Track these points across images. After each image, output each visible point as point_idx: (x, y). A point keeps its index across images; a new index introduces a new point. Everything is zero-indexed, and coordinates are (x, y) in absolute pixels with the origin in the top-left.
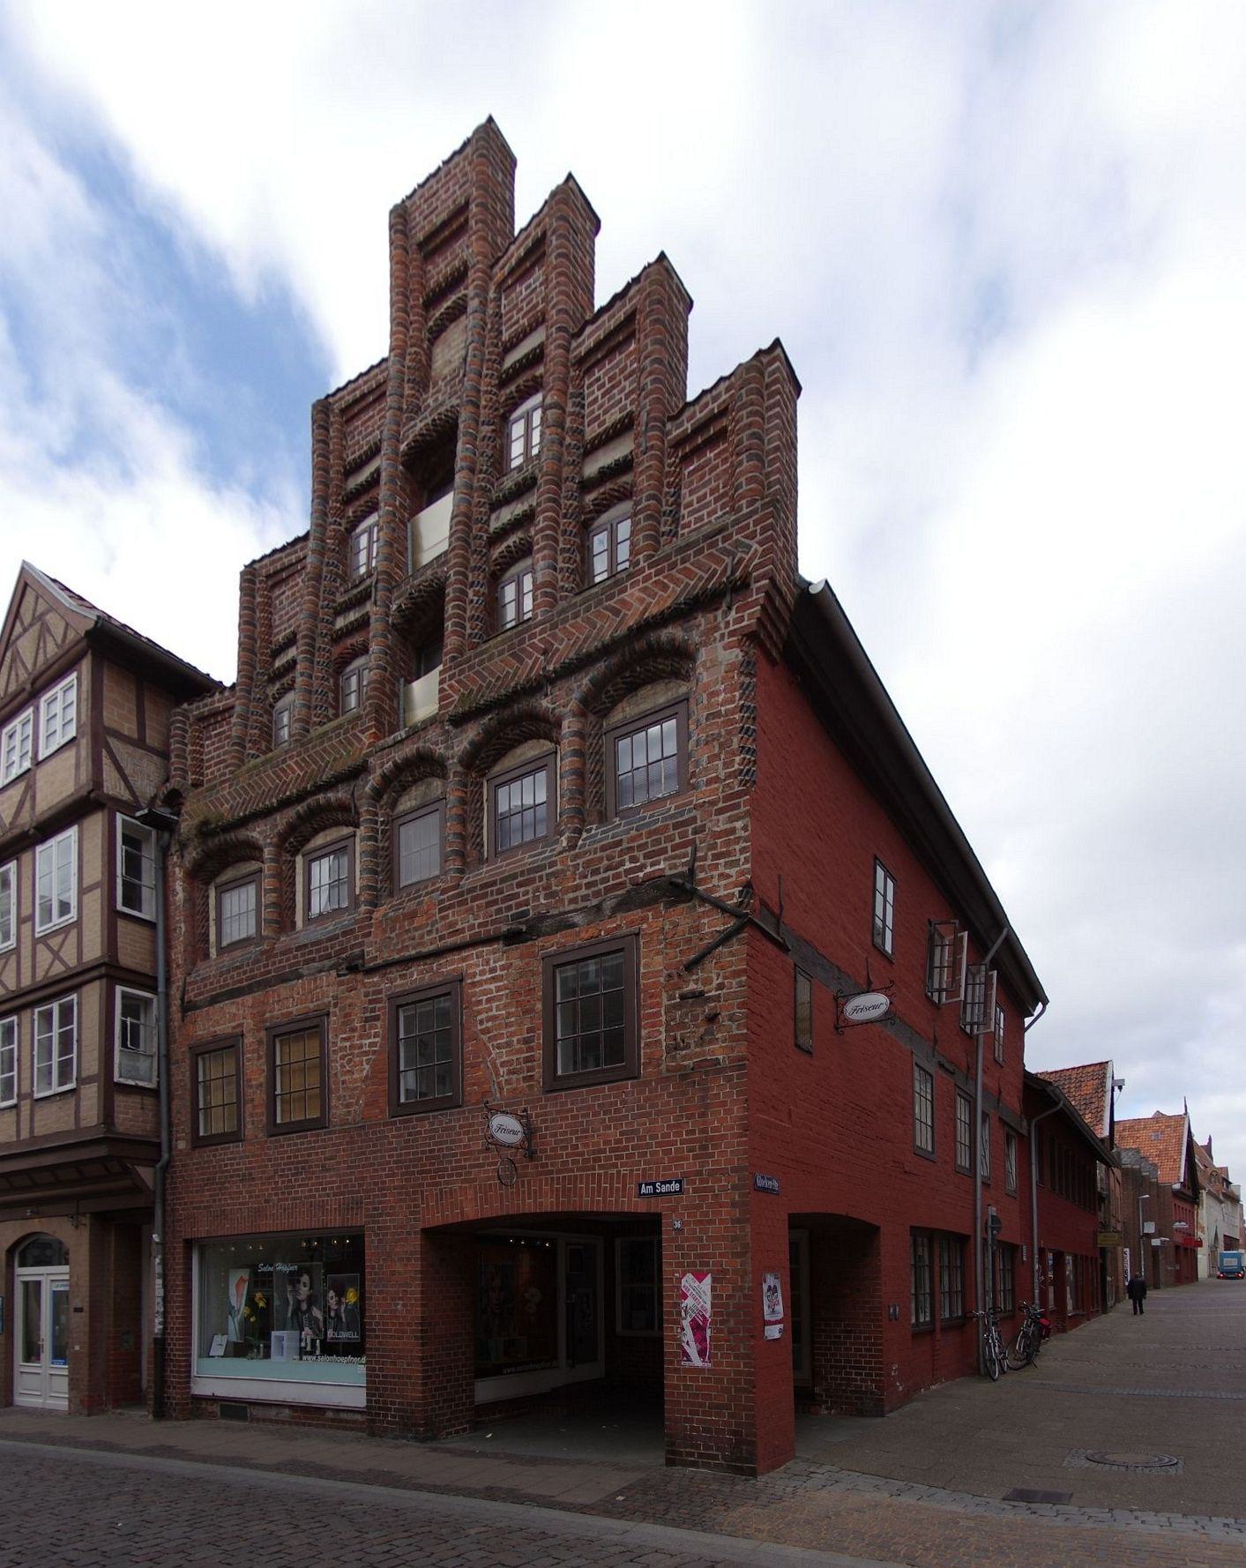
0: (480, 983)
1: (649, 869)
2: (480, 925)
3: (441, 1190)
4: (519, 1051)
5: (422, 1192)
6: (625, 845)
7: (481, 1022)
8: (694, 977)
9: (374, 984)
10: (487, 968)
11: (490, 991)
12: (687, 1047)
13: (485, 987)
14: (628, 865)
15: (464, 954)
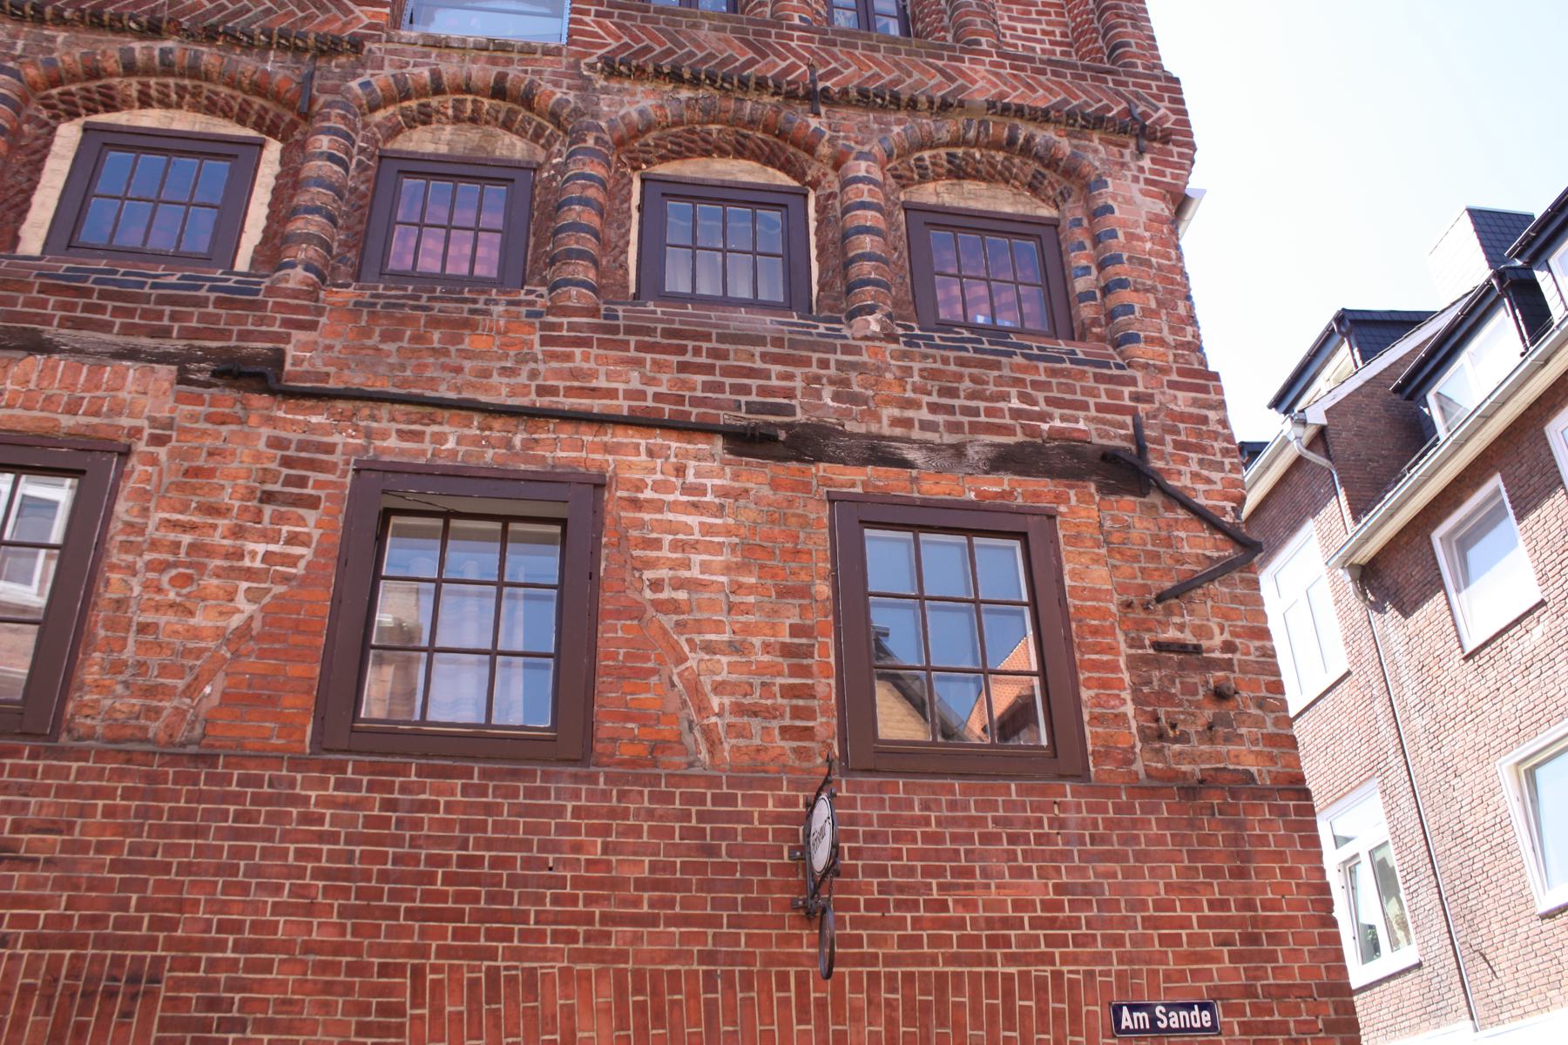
0: (658, 506)
1: (1057, 423)
2: (658, 397)
3: (493, 974)
4: (762, 669)
5: (418, 973)
6: (1006, 372)
7: (656, 585)
8: (1177, 620)
9: (313, 429)
10: (678, 483)
11: (688, 529)
12: (1183, 738)
13: (670, 516)
14: (1015, 403)
15: (611, 436)
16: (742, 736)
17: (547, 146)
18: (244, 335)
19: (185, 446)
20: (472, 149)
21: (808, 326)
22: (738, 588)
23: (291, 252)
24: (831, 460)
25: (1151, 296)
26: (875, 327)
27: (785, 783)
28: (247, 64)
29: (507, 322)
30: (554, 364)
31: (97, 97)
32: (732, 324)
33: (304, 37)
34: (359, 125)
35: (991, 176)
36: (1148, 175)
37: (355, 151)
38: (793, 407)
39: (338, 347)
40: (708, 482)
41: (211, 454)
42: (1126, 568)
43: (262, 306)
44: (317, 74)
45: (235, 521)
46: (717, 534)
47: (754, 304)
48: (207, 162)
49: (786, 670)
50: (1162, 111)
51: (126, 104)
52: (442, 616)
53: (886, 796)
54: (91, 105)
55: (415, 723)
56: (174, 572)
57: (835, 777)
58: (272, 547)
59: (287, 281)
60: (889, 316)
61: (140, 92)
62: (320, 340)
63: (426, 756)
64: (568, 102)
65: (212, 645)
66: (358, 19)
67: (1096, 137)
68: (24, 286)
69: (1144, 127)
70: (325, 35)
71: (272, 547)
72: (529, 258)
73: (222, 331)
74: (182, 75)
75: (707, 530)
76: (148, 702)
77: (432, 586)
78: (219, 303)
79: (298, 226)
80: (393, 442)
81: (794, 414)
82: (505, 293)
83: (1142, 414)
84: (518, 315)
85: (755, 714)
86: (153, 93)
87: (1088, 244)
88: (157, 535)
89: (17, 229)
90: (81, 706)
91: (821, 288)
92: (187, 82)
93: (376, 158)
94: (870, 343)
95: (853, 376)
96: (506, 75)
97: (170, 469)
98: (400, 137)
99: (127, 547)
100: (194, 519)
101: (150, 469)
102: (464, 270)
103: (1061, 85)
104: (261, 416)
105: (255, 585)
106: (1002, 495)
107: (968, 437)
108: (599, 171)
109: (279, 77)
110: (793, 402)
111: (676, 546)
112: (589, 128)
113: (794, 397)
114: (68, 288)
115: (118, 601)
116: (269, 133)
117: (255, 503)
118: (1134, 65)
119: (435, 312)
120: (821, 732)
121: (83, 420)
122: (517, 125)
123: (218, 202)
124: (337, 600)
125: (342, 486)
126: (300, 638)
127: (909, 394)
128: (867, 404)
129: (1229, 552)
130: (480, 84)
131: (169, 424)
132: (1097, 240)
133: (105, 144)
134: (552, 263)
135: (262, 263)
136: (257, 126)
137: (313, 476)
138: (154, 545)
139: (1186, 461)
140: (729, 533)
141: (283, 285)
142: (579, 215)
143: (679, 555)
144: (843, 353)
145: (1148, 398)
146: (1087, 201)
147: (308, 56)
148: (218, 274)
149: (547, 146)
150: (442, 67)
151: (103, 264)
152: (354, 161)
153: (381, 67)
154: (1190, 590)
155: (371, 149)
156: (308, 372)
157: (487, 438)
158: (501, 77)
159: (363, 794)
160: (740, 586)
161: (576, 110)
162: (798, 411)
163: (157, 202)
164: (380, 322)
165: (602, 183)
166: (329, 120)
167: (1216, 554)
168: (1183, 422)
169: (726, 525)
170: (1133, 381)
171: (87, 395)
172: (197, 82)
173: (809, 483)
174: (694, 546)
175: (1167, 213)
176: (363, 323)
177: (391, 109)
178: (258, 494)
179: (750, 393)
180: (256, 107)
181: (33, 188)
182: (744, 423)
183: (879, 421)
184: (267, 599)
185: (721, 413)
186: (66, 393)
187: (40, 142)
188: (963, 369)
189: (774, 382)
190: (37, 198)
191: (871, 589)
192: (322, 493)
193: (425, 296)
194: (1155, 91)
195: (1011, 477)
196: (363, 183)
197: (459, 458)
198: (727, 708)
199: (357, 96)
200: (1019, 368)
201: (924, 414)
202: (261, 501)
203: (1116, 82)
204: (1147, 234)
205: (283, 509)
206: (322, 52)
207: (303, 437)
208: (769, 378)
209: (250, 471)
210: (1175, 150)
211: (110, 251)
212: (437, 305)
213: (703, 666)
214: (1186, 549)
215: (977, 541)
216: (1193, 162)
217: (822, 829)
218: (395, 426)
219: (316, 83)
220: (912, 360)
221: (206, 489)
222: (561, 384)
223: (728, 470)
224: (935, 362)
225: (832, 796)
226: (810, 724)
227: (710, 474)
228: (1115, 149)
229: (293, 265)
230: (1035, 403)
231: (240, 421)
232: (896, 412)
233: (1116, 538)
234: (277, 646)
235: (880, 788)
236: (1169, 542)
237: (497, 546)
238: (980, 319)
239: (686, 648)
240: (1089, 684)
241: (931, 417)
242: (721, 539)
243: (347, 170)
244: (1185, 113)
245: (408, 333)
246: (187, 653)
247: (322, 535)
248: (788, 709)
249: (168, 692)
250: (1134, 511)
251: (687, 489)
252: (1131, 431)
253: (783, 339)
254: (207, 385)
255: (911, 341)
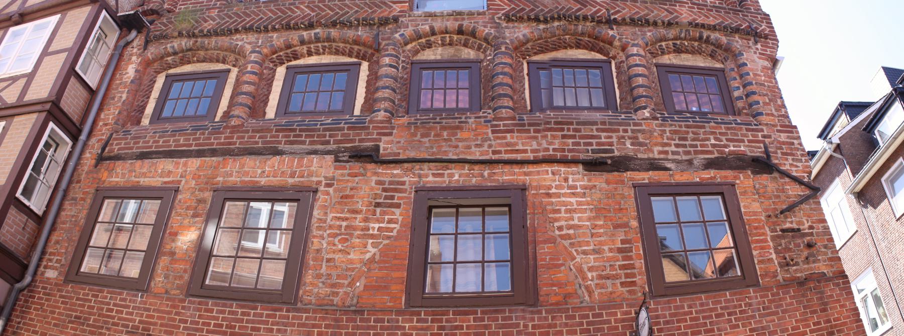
4: (609, 259)
8: (789, 220)
11: (571, 204)
16: (603, 288)
17: (484, 52)
18: (361, 141)
19: (341, 187)
20: (451, 56)
21: (617, 116)
22: (595, 226)
23: (378, 105)
24: (633, 170)
25: (766, 97)
26: (647, 115)
27: (625, 305)
28: (350, 34)
29: (476, 125)
30: (499, 141)
31: (291, 55)
32: (581, 117)
33: (373, 19)
34: (401, 52)
35: (693, 52)
36: (760, 51)
37: (400, 62)
38: (613, 150)
39: (402, 142)
40: (578, 184)
41: (351, 189)
42: (767, 202)
43: (368, 128)
44: (380, 33)
45: (364, 215)
46: (584, 205)
47: (591, 108)
48: (337, 74)
49: (621, 258)
50: (763, 27)
51: (303, 56)
52: (459, 249)
53: (672, 305)
54: (289, 59)
55: (450, 293)
56: (340, 237)
57: (647, 300)
58: (381, 225)
59: (377, 117)
60: (653, 109)
61: (308, 51)
62: (394, 139)
63: (456, 307)
64: (491, 33)
65: (358, 266)
66: (395, 9)
67: (737, 36)
68: (270, 131)
69: (756, 33)
70: (382, 17)
71: (381, 225)
72: (482, 98)
73: (351, 140)
74: (324, 42)
75: (579, 203)
76: (333, 290)
77: (454, 236)
78: (349, 128)
79: (379, 94)
80: (431, 178)
81: (614, 153)
82: (473, 114)
83: (767, 143)
84: (480, 122)
85: (608, 278)
86: (313, 50)
87: (738, 78)
88: (332, 223)
89: (265, 110)
90: (305, 292)
91: (621, 100)
92: (326, 44)
93: (410, 64)
94: (646, 121)
95: (639, 135)
96: (463, 25)
97: (335, 196)
98: (419, 54)
99: (319, 228)
100: (346, 215)
101: (326, 197)
102: (454, 105)
103: (719, 15)
104: (372, 172)
105: (375, 241)
106: (711, 178)
107: (693, 156)
108: (509, 61)
109: (364, 37)
110: (613, 148)
111: (567, 211)
112: (502, 43)
113: (613, 145)
114: (287, 129)
115: (317, 250)
116: (363, 59)
117: (373, 207)
118: (750, 9)
119: (444, 124)
120: (639, 282)
121: (297, 179)
122: (470, 45)
123: (344, 89)
124: (412, 245)
125: (410, 198)
126: (397, 262)
127: (666, 141)
128: (646, 146)
129: (808, 192)
130: (452, 30)
131: (333, 178)
132: (741, 76)
133: (296, 73)
134: (493, 99)
135: (365, 111)
136: (357, 57)
137: (397, 195)
138: (331, 227)
139: (787, 160)
140: (588, 204)
141: (376, 119)
142: (502, 79)
143: (568, 215)
144: (634, 126)
145: (769, 137)
146: (736, 61)
147: (376, 27)
148: (347, 117)
149: (484, 52)
150: (434, 24)
151: (299, 119)
152: (401, 66)
153: (408, 27)
154: (794, 208)
155: (407, 60)
156: (390, 153)
157: (472, 174)
158: (461, 26)
159: (429, 324)
160: (596, 226)
161: (495, 37)
162: (616, 151)
163: (319, 92)
164: (420, 130)
165: (511, 65)
166: (388, 51)
167: (802, 194)
168: (784, 145)
169: (587, 201)
170: (762, 130)
171: (298, 170)
172: (330, 43)
173: (624, 180)
174: (575, 211)
175: (769, 65)
176: (412, 131)
177: (414, 44)
178: (374, 204)
179: (593, 145)
180: (356, 49)
181: (269, 93)
182: (591, 158)
183: (653, 152)
184: (381, 246)
185: (581, 154)
186: (289, 170)
187: (271, 76)
188: (688, 129)
189: (603, 140)
190: (271, 97)
191: (656, 221)
192: (401, 202)
193: (438, 118)
194: (760, 19)
195: (714, 171)
196: (405, 74)
197: (461, 183)
198: (595, 277)
199: (399, 40)
200: (713, 127)
201: (673, 148)
202: (375, 207)
203: (743, 15)
204: (762, 74)
205: (385, 209)
206: (381, 24)
207: (391, 179)
208: (601, 138)
209: (369, 195)
210: (770, 42)
211: (302, 113)
212: (444, 121)
213: (583, 260)
214: (791, 193)
215: (702, 197)
216: (778, 47)
217: (644, 322)
218: (431, 172)
219: (380, 37)
220: (665, 127)
221: (351, 204)
222: (503, 149)
223: (585, 178)
224: (676, 127)
225: (647, 308)
226: (634, 280)
227: (578, 180)
228: (745, 41)
229: (379, 111)
230: (722, 141)
231: (363, 175)
232: (660, 149)
233: (761, 191)
234: (387, 265)
235: (669, 302)
236: (783, 191)
237: (481, 218)
238: (694, 109)
239: (575, 254)
240: (756, 249)
241: (676, 149)
242: (585, 207)
243: (398, 70)
244: (773, 28)
245: (433, 133)
246: (348, 269)
247: (403, 219)
248: (623, 275)
249: (342, 285)
250: (768, 180)
251: (569, 187)
252: (763, 150)
253: (605, 122)
254: (347, 162)
255: (664, 119)
